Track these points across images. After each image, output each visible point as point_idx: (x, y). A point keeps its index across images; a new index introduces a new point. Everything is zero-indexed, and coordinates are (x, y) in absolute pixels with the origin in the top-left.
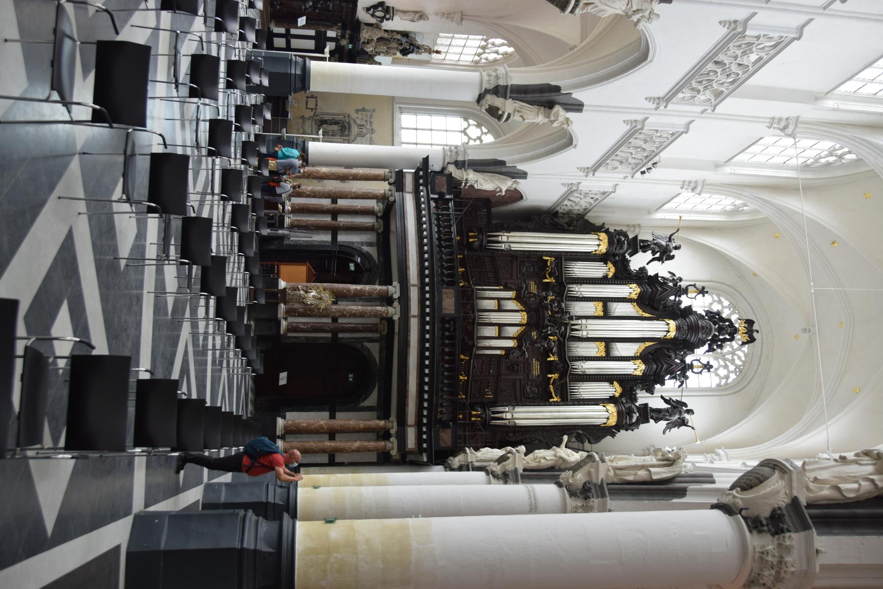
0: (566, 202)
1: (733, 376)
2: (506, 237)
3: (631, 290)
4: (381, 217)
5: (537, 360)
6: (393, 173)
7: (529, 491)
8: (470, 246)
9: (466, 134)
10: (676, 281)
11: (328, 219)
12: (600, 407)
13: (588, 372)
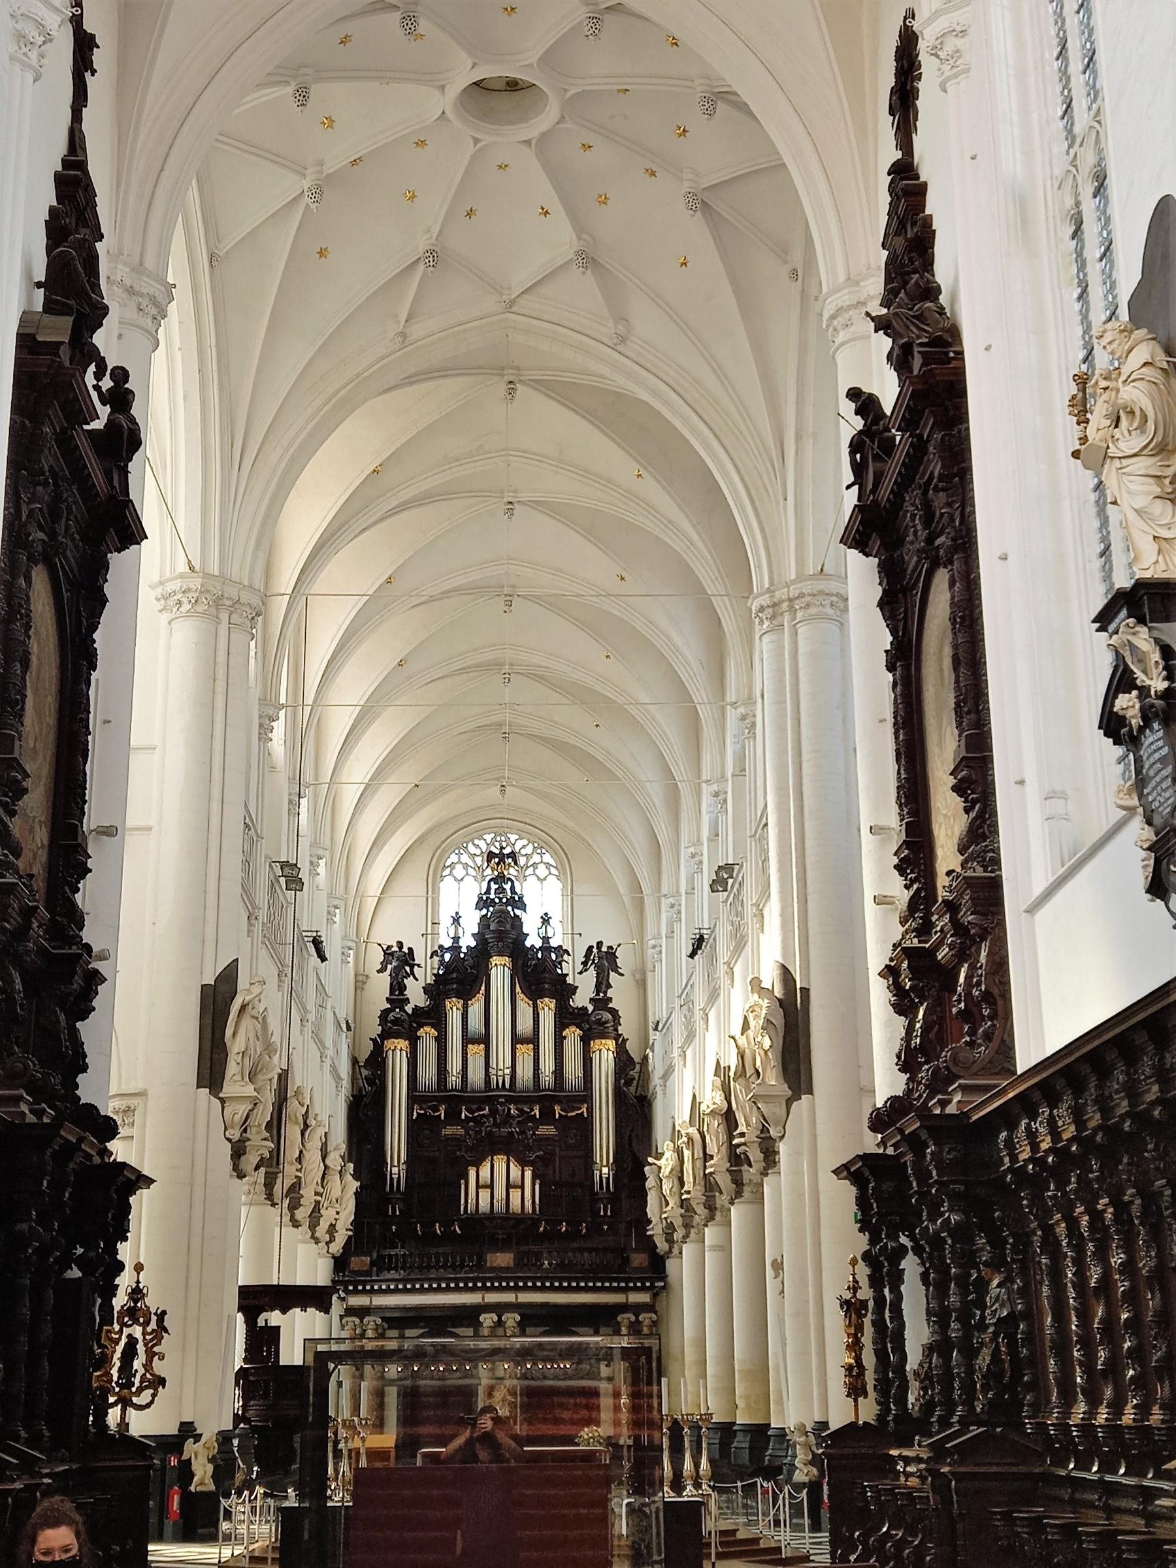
3: (453, 1010)
13: (552, 1068)
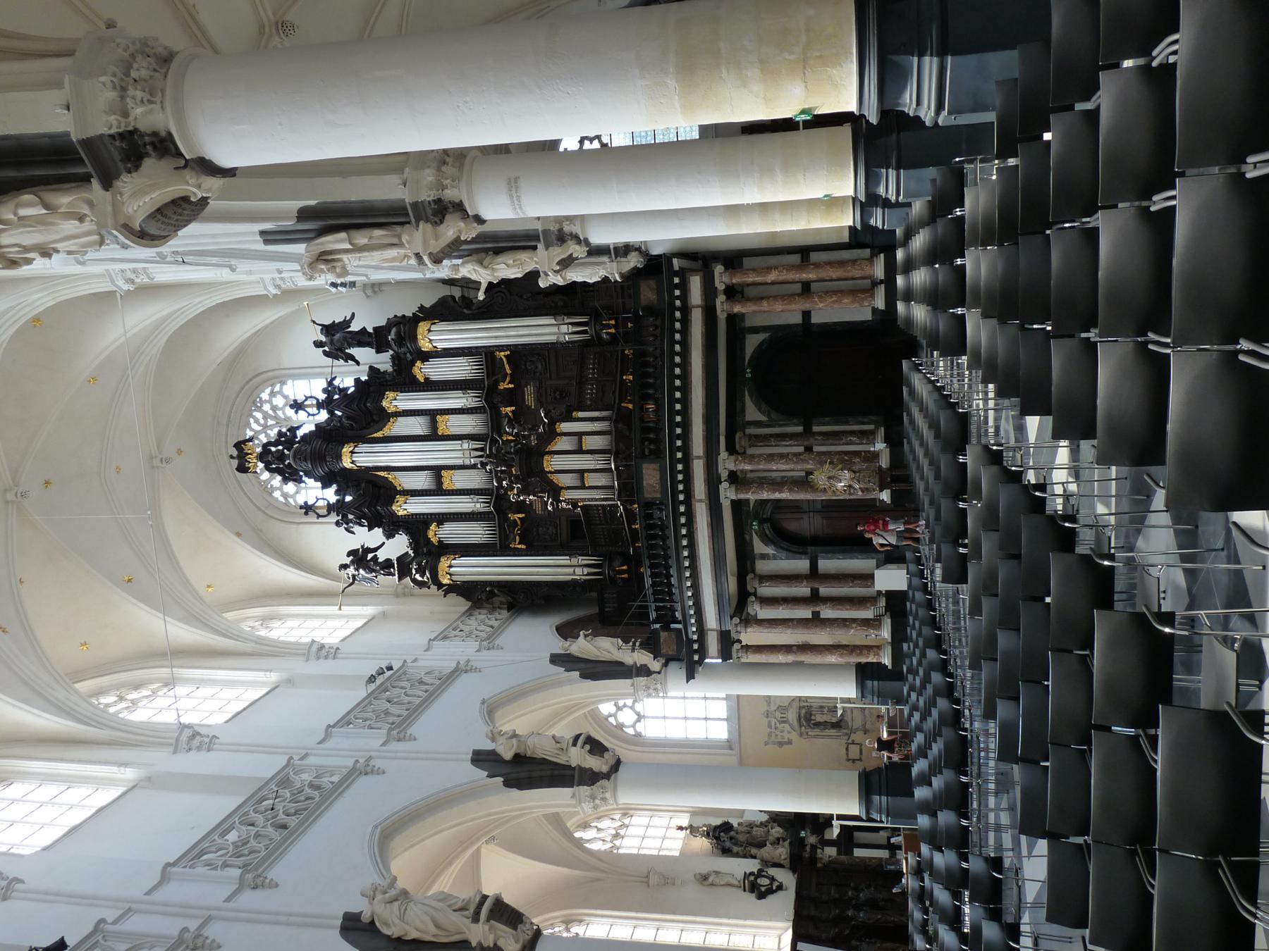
0: (496, 624)
1: (265, 396)
2: (577, 573)
3: (406, 507)
4: (750, 594)
5: (529, 407)
6: (736, 657)
7: (520, 208)
8: (626, 559)
9: (638, 714)
10: (344, 522)
11: (824, 591)
12: (441, 346)
13: (459, 393)
